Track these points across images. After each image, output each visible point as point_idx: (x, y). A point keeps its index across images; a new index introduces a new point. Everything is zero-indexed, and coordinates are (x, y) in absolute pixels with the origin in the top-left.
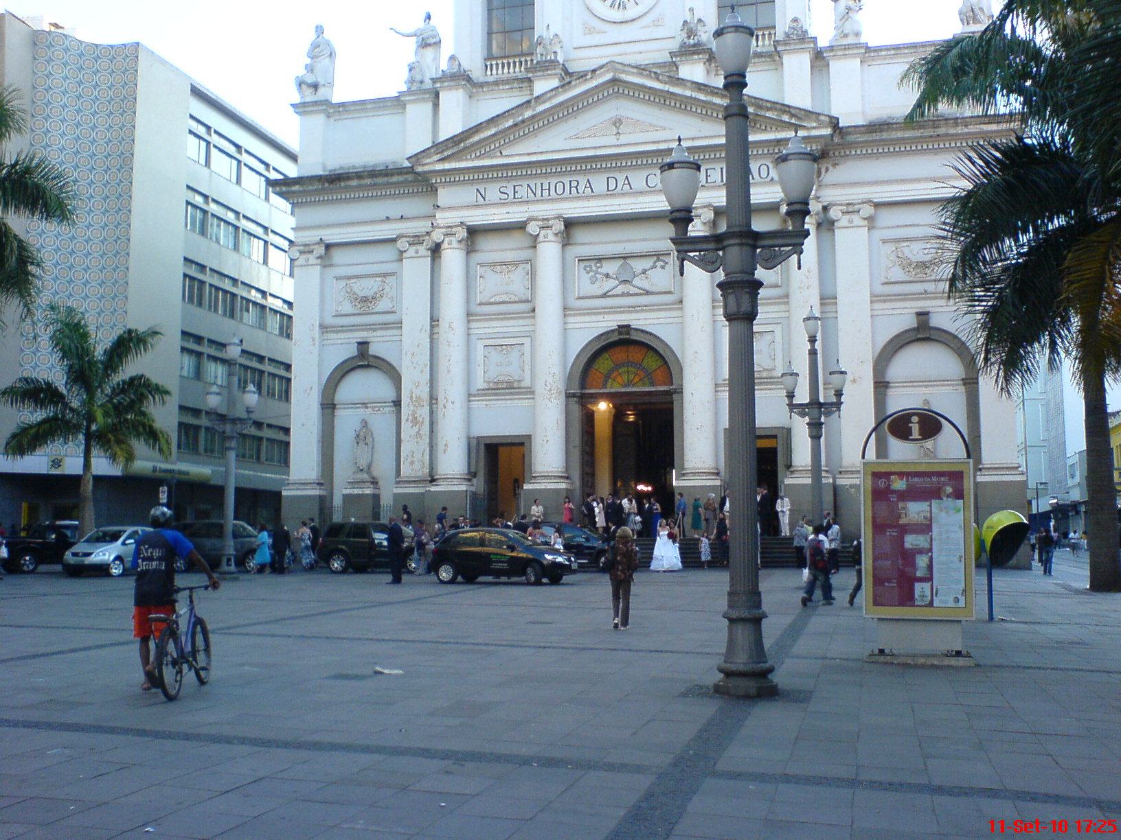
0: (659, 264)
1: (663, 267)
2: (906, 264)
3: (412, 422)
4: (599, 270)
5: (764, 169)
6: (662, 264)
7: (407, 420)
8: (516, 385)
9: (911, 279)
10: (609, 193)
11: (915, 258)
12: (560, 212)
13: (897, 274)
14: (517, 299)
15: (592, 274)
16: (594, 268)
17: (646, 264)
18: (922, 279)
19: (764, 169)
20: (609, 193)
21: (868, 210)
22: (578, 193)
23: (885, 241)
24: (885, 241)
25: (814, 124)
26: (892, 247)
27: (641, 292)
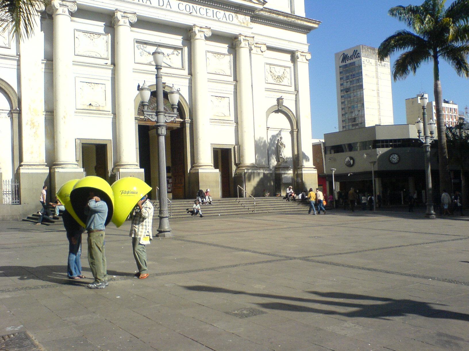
0: (176, 52)
1: (177, 55)
2: (273, 76)
3: (30, 125)
4: (145, 49)
5: (231, 16)
6: (177, 53)
7: (27, 124)
8: (101, 108)
9: (275, 83)
10: (159, 7)
11: (277, 74)
12: (135, 11)
13: (271, 80)
14: (99, 56)
15: (141, 50)
16: (142, 47)
17: (170, 51)
18: (279, 84)
19: (231, 16)
20: (159, 7)
21: (264, 48)
22: (143, 2)
23: (267, 64)
24: (267, 64)
25: (257, 2)
26: (268, 67)
27: (168, 66)
